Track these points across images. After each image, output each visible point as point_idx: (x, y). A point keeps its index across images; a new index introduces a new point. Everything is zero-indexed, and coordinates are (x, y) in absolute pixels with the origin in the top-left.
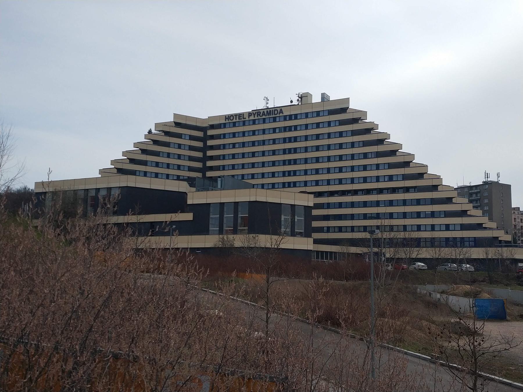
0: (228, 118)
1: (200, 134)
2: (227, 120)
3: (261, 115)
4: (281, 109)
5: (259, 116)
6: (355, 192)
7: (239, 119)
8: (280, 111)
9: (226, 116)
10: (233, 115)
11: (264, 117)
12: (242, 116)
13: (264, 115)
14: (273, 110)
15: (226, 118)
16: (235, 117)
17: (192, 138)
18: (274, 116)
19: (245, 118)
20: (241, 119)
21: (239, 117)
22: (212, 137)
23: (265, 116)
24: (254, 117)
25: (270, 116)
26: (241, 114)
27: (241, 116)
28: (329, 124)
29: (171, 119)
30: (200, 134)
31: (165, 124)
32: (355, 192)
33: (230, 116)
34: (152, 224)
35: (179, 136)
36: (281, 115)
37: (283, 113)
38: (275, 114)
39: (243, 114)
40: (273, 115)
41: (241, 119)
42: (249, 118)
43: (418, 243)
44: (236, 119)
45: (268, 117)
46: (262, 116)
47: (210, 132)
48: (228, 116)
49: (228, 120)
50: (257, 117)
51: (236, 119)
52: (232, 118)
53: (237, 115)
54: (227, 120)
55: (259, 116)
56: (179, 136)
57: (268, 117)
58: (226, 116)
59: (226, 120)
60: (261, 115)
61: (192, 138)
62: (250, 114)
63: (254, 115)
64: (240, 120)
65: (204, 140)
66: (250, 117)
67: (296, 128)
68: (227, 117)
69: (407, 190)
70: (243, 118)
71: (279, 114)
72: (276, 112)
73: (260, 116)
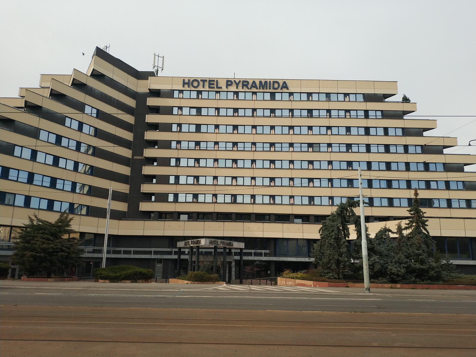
0: (188, 84)
1: (131, 103)
2: (186, 86)
3: (249, 86)
4: (285, 83)
5: (245, 87)
7: (209, 87)
8: (283, 84)
9: (184, 80)
10: (199, 80)
11: (254, 90)
12: (215, 84)
13: (254, 87)
14: (270, 82)
15: (184, 83)
16: (201, 83)
18: (270, 91)
19: (221, 88)
20: (214, 88)
21: (210, 84)
23: (257, 88)
24: (237, 88)
25: (265, 91)
26: (214, 81)
27: (213, 84)
29: (70, 72)
30: (131, 103)
31: (54, 78)
33: (192, 80)
36: (285, 90)
37: (288, 89)
38: (274, 88)
39: (217, 81)
40: (270, 89)
41: (214, 88)
42: (227, 88)
44: (203, 87)
45: (261, 90)
46: (251, 88)
47: (152, 102)
48: (189, 80)
49: (189, 87)
50: (243, 88)
51: (203, 87)
52: (195, 84)
53: (206, 81)
54: (186, 86)
55: (245, 87)
57: (261, 90)
58: (184, 80)
59: (183, 86)
60: (249, 86)
62: (229, 83)
63: (237, 85)
64: (210, 90)
66: (229, 87)
68: (186, 81)
70: (217, 87)
71: (281, 89)
72: (276, 86)
73: (248, 88)
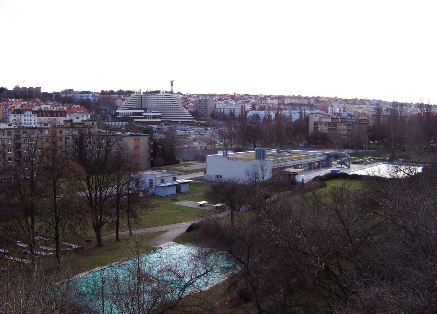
1: (140, 97)
6: (169, 110)
17: (139, 98)
22: (143, 98)
28: (165, 98)
30: (140, 97)
32: (169, 110)
34: (138, 117)
35: (137, 98)
43: (180, 119)
47: (142, 97)
56: (137, 98)
61: (139, 98)
65: (141, 98)
67: (159, 98)
69: (177, 110)
